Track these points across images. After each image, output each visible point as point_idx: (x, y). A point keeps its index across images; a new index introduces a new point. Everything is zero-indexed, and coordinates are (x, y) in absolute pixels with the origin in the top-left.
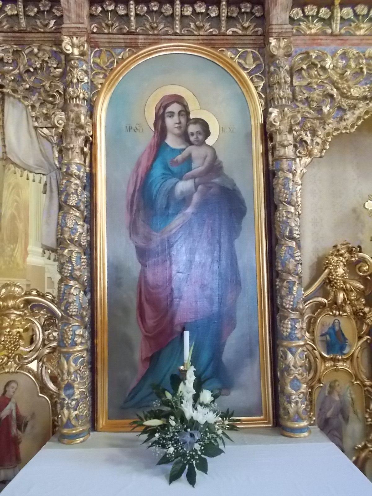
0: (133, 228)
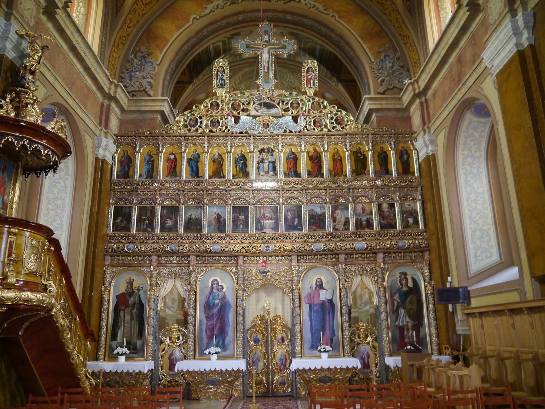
0: (205, 312)
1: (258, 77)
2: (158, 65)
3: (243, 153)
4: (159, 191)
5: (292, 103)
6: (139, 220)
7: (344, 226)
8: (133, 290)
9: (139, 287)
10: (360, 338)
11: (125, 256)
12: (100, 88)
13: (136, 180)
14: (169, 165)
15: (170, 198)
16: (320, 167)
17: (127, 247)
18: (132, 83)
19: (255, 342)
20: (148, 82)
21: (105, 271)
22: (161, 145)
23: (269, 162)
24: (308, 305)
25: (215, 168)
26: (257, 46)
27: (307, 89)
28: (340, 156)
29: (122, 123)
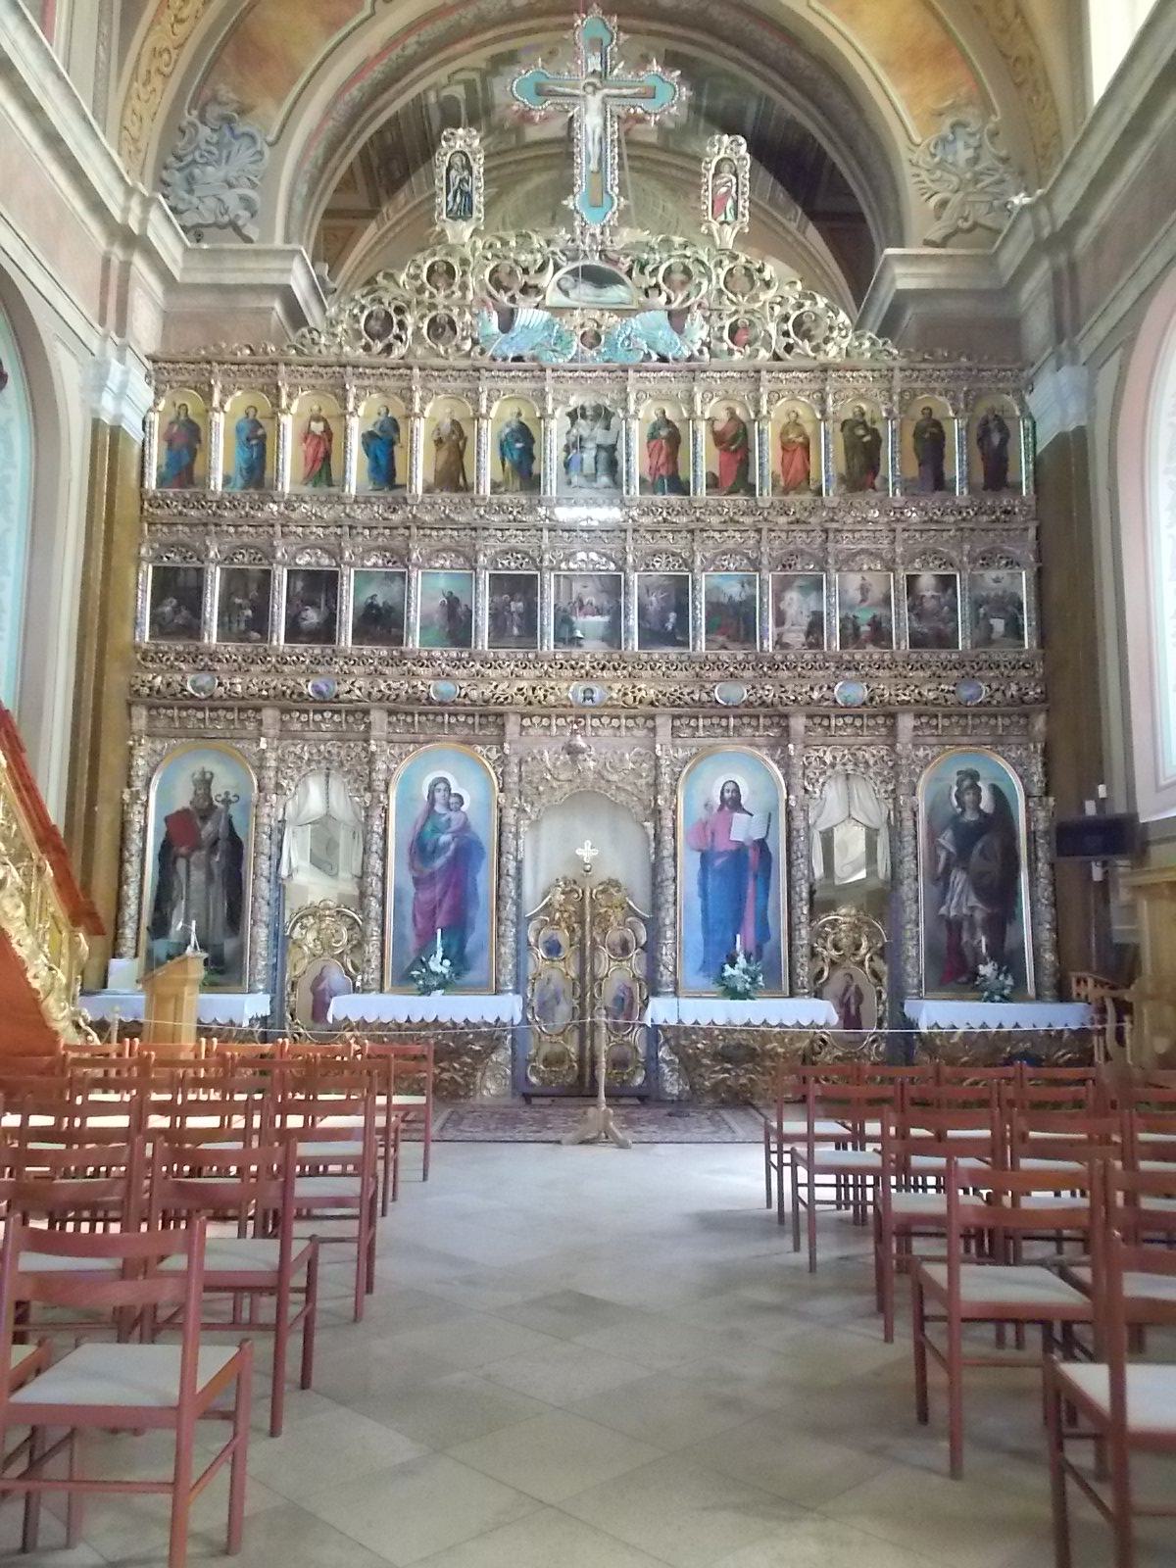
0: (412, 867)
1: (568, 188)
2: (271, 145)
3: (522, 419)
4: (283, 526)
5: (669, 270)
6: (227, 609)
7: (807, 636)
8: (211, 804)
9: (227, 793)
10: (837, 949)
11: (187, 708)
12: (97, 207)
13: (214, 493)
14: (311, 450)
15: (313, 547)
16: (745, 464)
17: (194, 682)
18: (195, 201)
19: (549, 951)
20: (244, 199)
21: (131, 748)
22: (284, 393)
23: (599, 447)
24: (698, 855)
25: (441, 462)
26: (568, 90)
27: (715, 226)
28: (802, 434)
29: (169, 320)
